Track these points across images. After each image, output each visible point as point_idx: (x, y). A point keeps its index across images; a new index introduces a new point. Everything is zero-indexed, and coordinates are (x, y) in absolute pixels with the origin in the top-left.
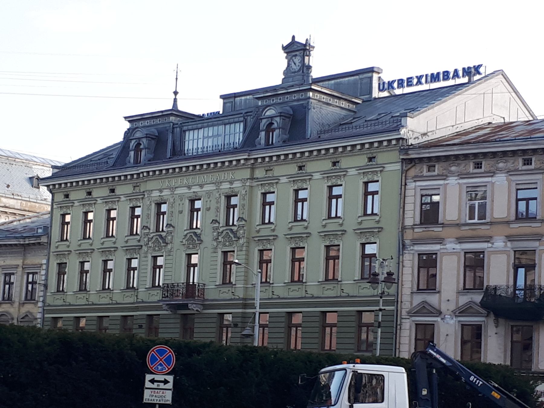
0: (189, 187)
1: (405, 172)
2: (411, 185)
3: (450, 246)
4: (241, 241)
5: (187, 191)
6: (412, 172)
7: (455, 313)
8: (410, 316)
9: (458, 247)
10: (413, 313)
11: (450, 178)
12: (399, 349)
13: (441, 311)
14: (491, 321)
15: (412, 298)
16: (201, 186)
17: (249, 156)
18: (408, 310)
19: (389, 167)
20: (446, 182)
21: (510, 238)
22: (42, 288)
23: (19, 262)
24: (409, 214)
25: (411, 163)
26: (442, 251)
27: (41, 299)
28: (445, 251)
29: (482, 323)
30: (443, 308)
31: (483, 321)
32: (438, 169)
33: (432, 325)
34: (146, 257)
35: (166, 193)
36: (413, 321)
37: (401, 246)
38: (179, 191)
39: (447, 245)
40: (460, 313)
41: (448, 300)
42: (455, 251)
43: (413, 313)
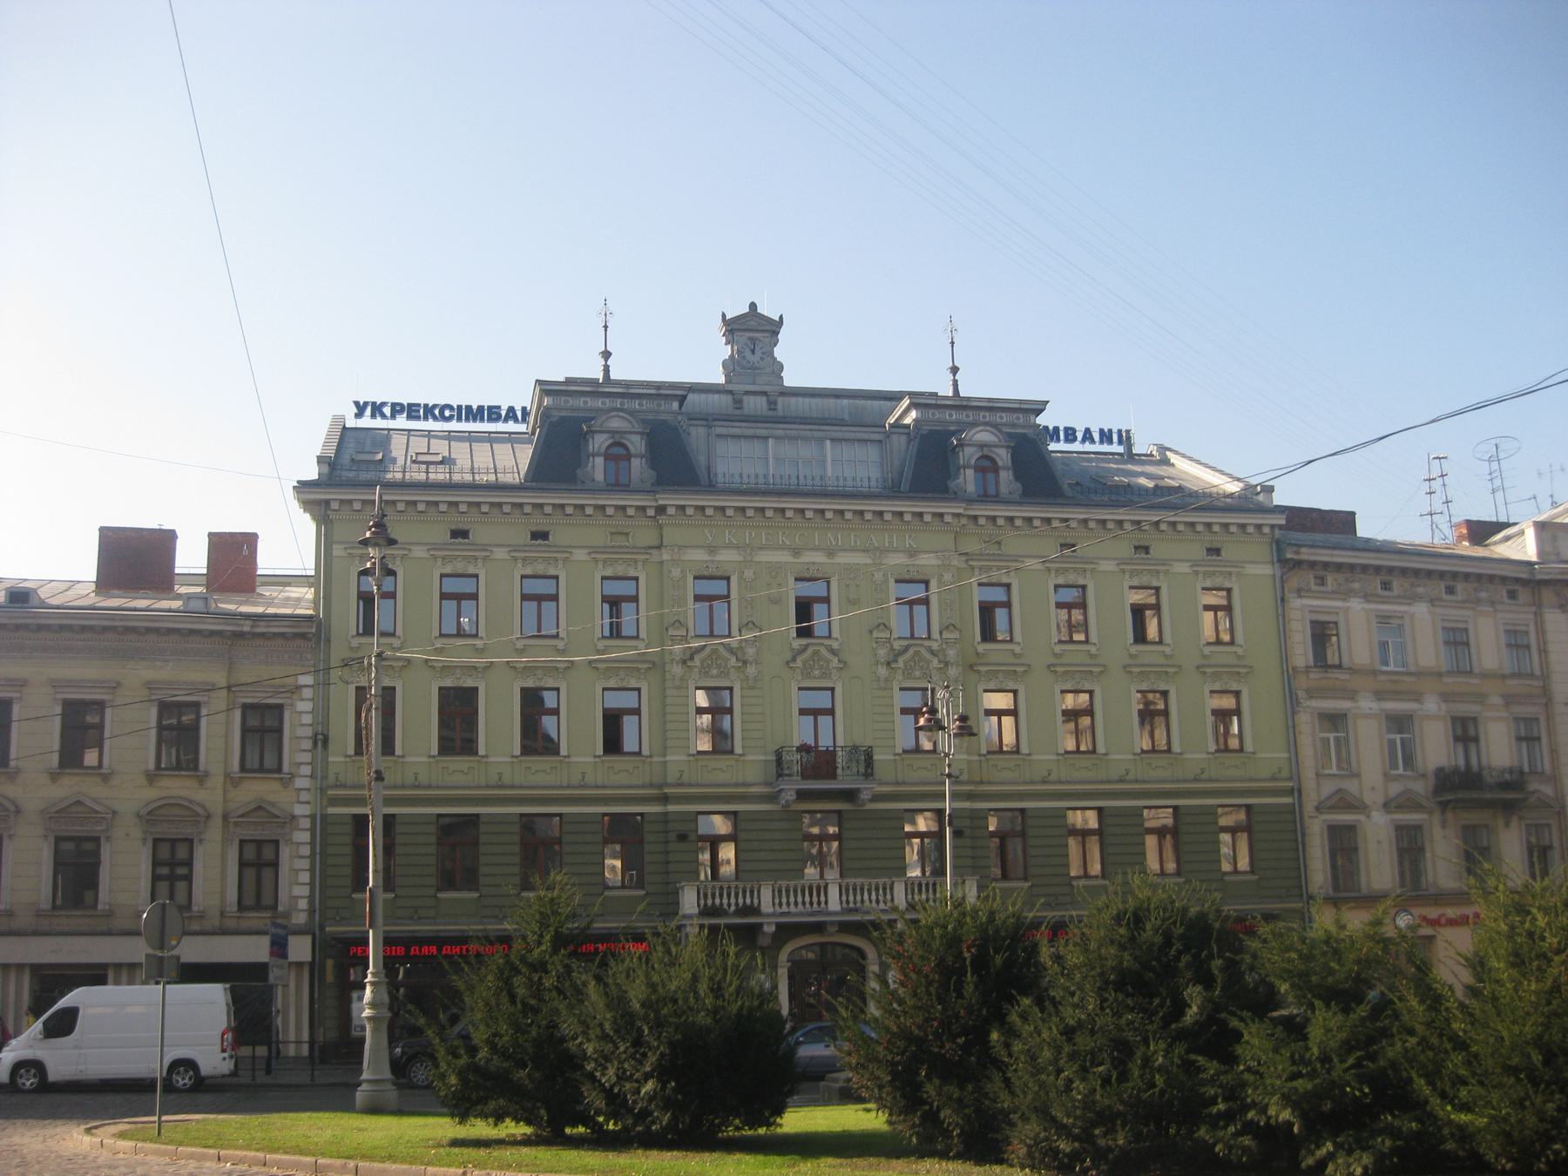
0: (796, 552)
4: (953, 672)
5: (791, 559)
6: (1294, 581)
14: (1436, 818)
15: (1318, 784)
16: (831, 553)
17: (965, 509)
18: (1315, 804)
19: (1252, 570)
20: (1348, 604)
21: (1446, 697)
22: (308, 744)
23: (220, 678)
25: (1294, 567)
27: (306, 770)
30: (1368, 798)
33: (1351, 829)
34: (679, 688)
35: (727, 556)
36: (1324, 821)
38: (765, 557)
40: (1396, 807)
42: (1373, 712)
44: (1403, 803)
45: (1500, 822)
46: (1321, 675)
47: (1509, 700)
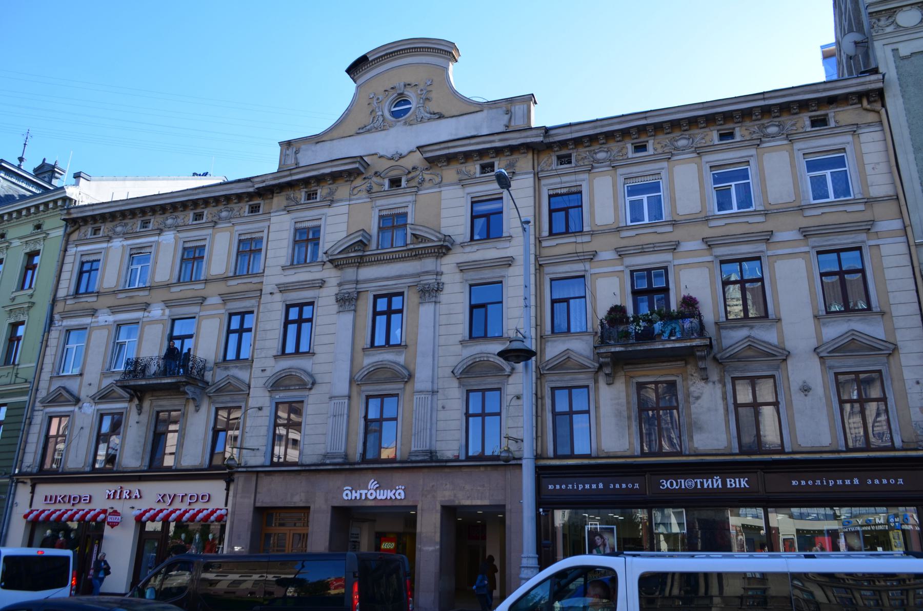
1: (67, 236)
2: (72, 250)
3: (105, 318)
7: (94, 399)
8: (44, 406)
9: (111, 318)
10: (49, 402)
11: (115, 240)
12: (24, 449)
13: (81, 397)
20: (110, 245)
21: (168, 304)
24: (64, 284)
26: (92, 325)
28: (96, 325)
29: (124, 411)
31: (124, 408)
32: (105, 229)
36: (46, 413)
37: (48, 322)
39: (99, 318)
40: (98, 399)
41: (90, 385)
42: (107, 323)
43: (49, 402)
44: (104, 396)
45: (191, 407)
46: (77, 300)
47: (226, 298)
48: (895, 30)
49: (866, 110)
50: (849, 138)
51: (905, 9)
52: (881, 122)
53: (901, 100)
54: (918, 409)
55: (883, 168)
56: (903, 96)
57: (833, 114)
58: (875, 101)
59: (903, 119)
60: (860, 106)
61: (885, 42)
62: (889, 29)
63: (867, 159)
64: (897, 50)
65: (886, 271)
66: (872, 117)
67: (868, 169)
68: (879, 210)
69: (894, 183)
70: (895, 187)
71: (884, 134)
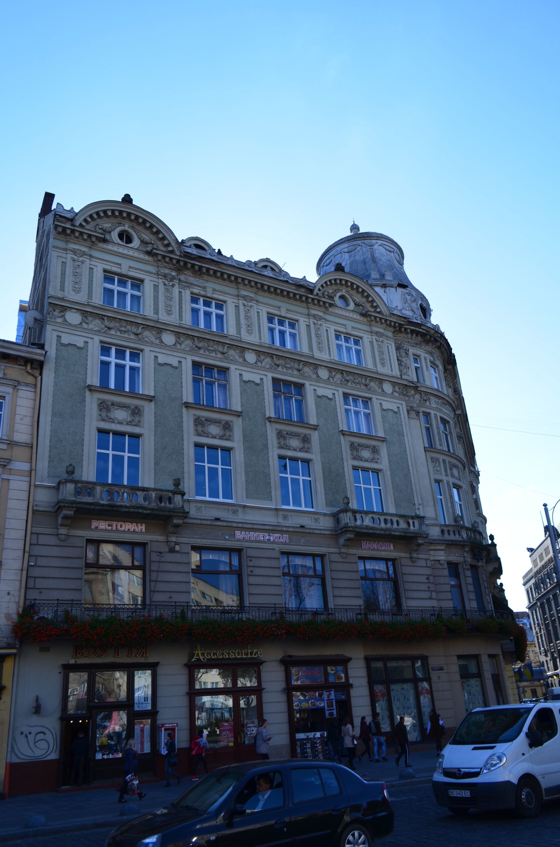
48: (63, 322)
49: (28, 372)
50: (10, 390)
51: (73, 310)
52: (36, 385)
53: (53, 375)
54: (3, 615)
55: (28, 420)
56: (55, 372)
57: (3, 367)
58: (36, 369)
59: (51, 389)
60: (24, 368)
61: (54, 328)
62: (59, 320)
63: (19, 410)
64: (60, 337)
65: (9, 501)
66: (30, 379)
67: (18, 418)
68: (18, 452)
69: (32, 434)
70: (33, 438)
71: (36, 395)
